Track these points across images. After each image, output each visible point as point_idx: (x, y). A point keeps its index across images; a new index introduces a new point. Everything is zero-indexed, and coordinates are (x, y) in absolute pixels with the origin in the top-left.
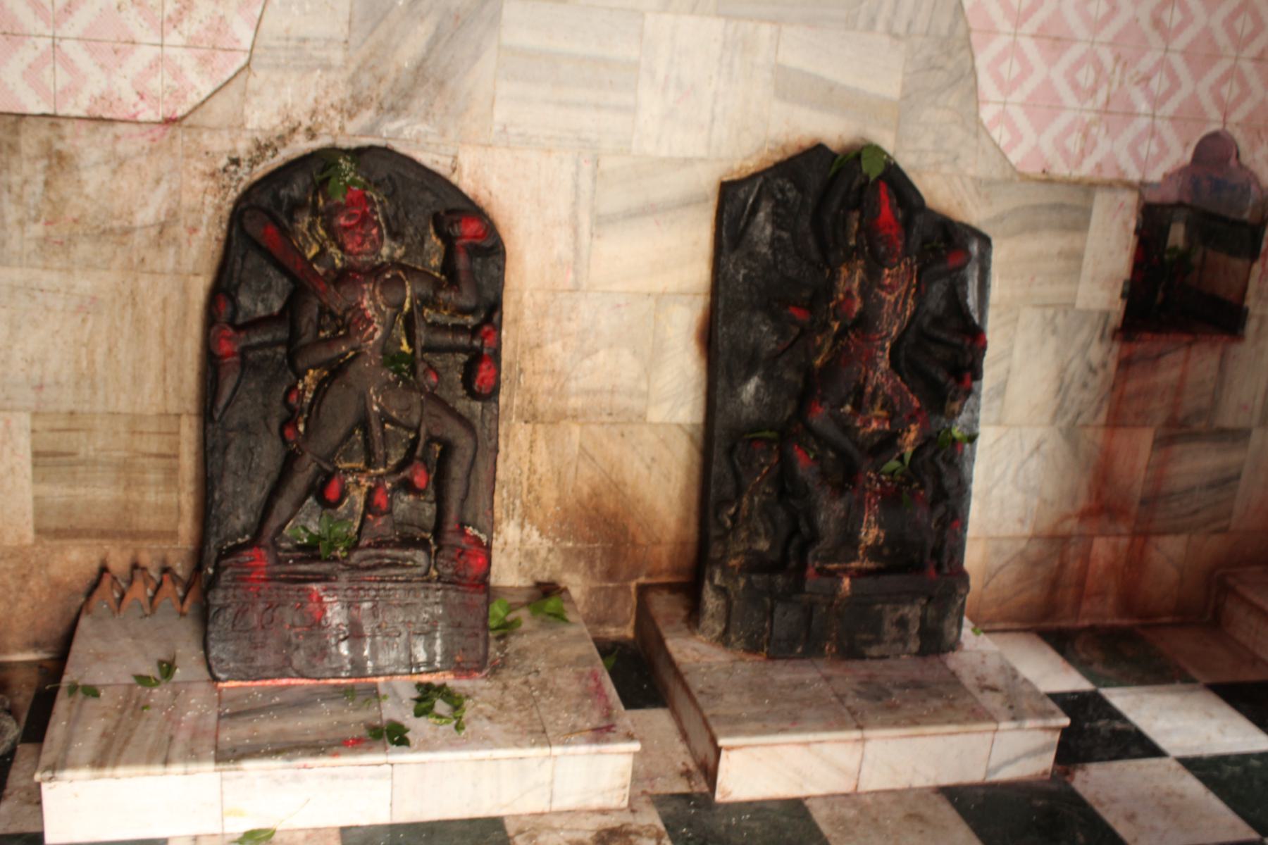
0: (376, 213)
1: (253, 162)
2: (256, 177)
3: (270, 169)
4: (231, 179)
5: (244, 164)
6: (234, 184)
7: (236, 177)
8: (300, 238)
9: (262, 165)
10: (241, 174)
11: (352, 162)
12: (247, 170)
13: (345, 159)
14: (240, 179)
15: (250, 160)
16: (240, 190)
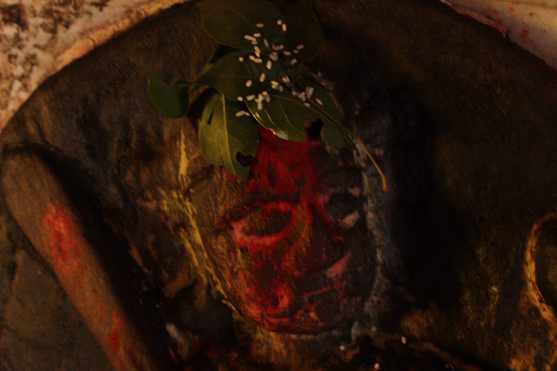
0: (356, 204)
1: (56, 21)
2: (68, 57)
3: (100, 36)
4: (11, 58)
5: (33, 22)
6: (19, 71)
7: (21, 55)
8: (151, 238)
9: (75, 28)
10: (29, 48)
11: (290, 41)
12: (43, 37)
13: (270, 33)
14: (31, 60)
15: (48, 13)
16: (33, 86)
